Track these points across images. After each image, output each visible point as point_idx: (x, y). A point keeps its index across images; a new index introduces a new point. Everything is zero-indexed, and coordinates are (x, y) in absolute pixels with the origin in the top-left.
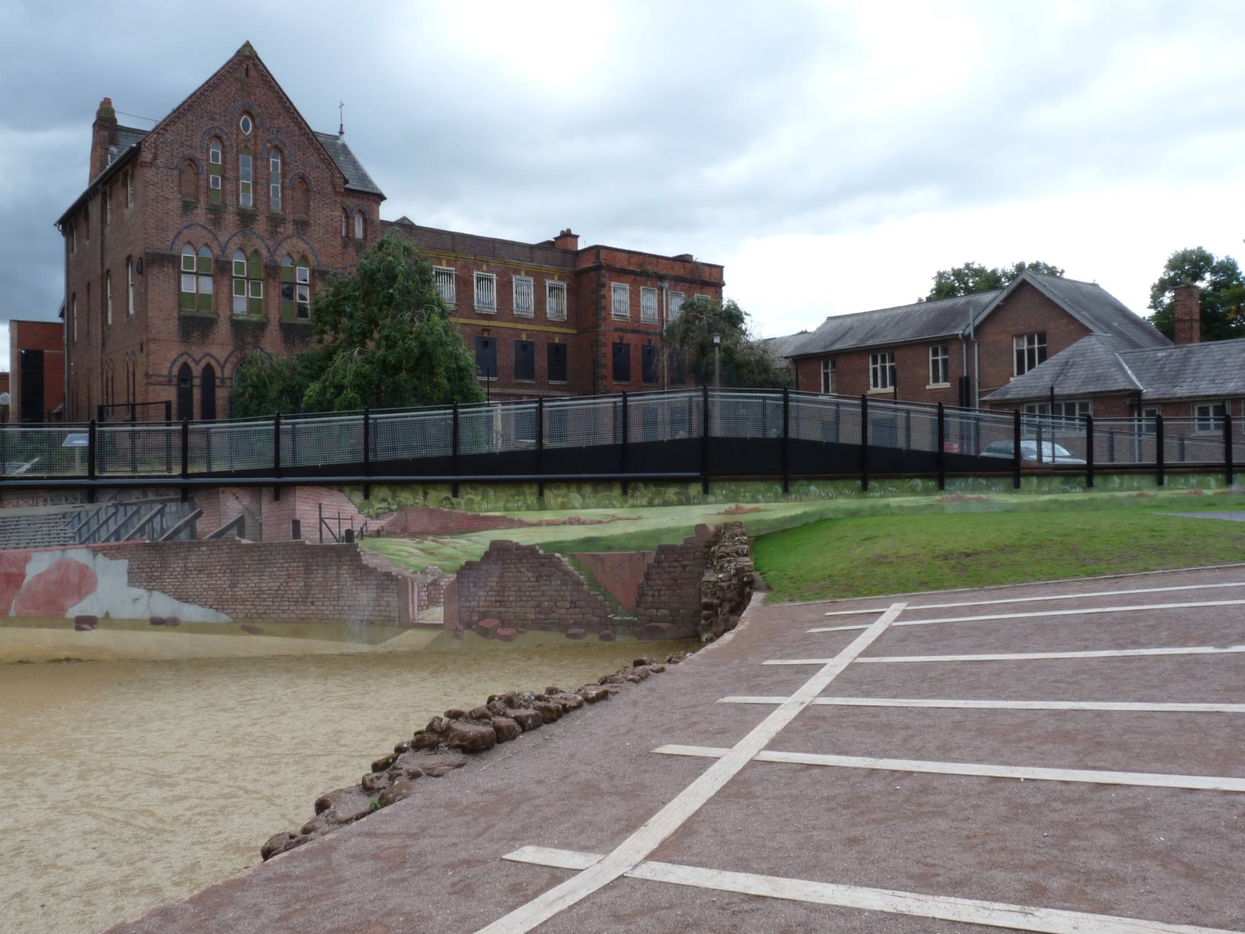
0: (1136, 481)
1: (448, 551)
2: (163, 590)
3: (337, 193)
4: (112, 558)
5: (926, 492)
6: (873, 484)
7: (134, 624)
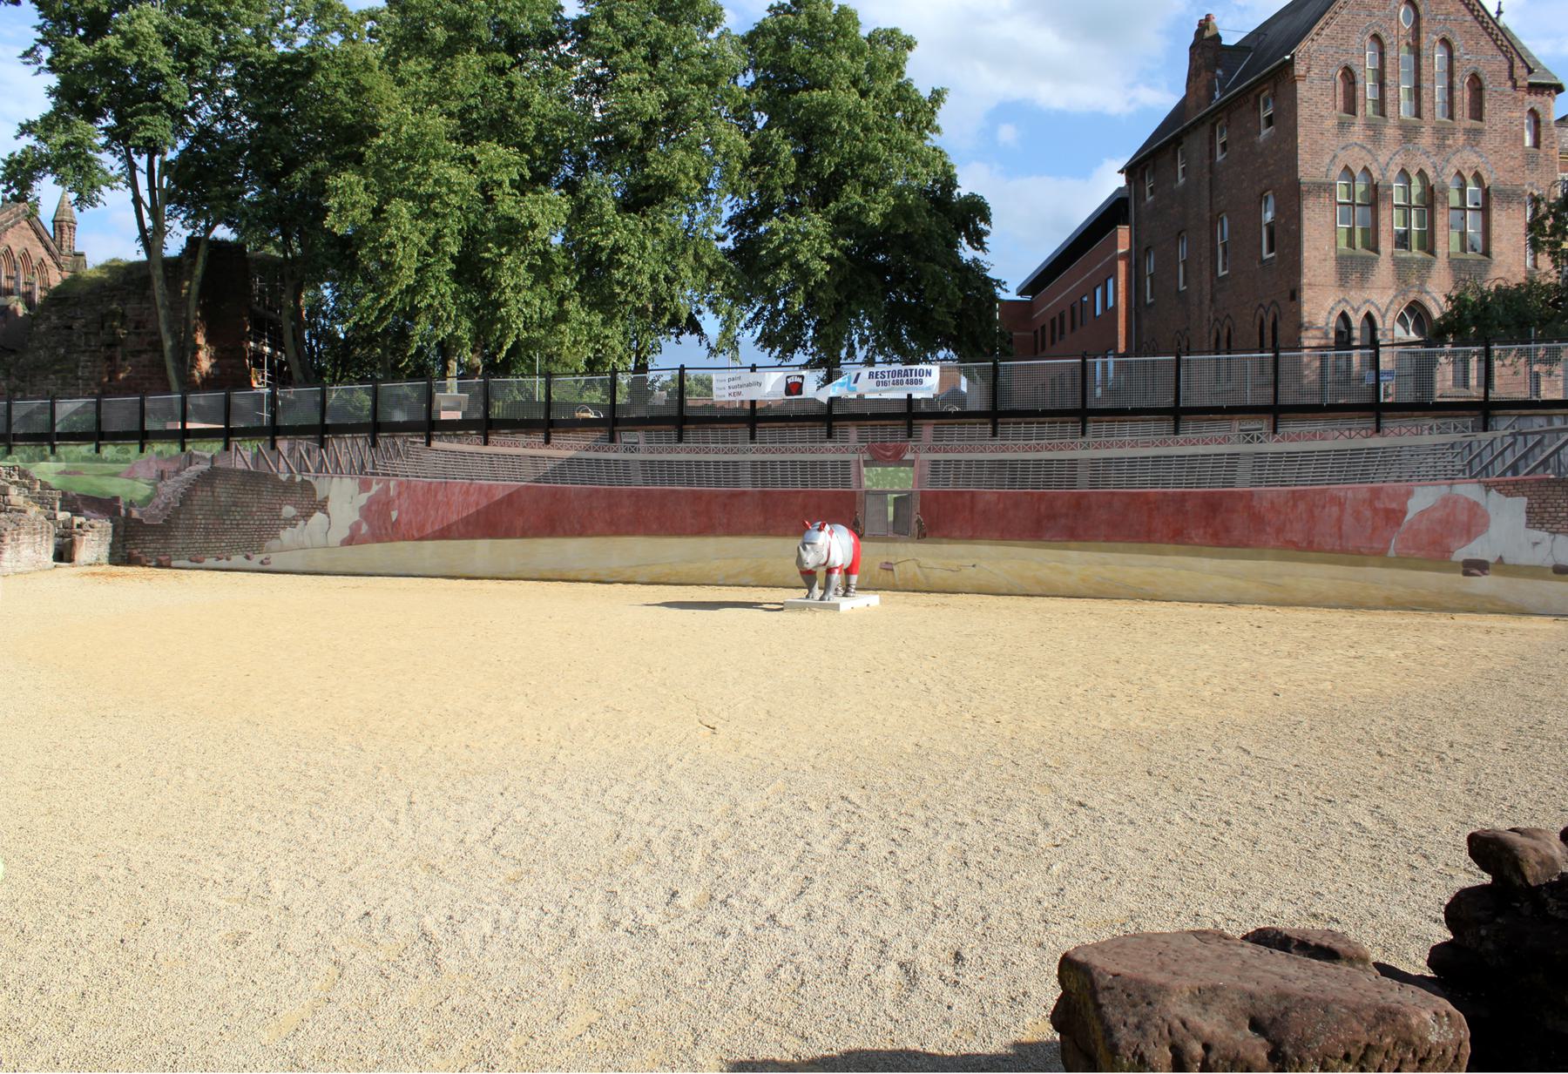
7: (1533, 572)
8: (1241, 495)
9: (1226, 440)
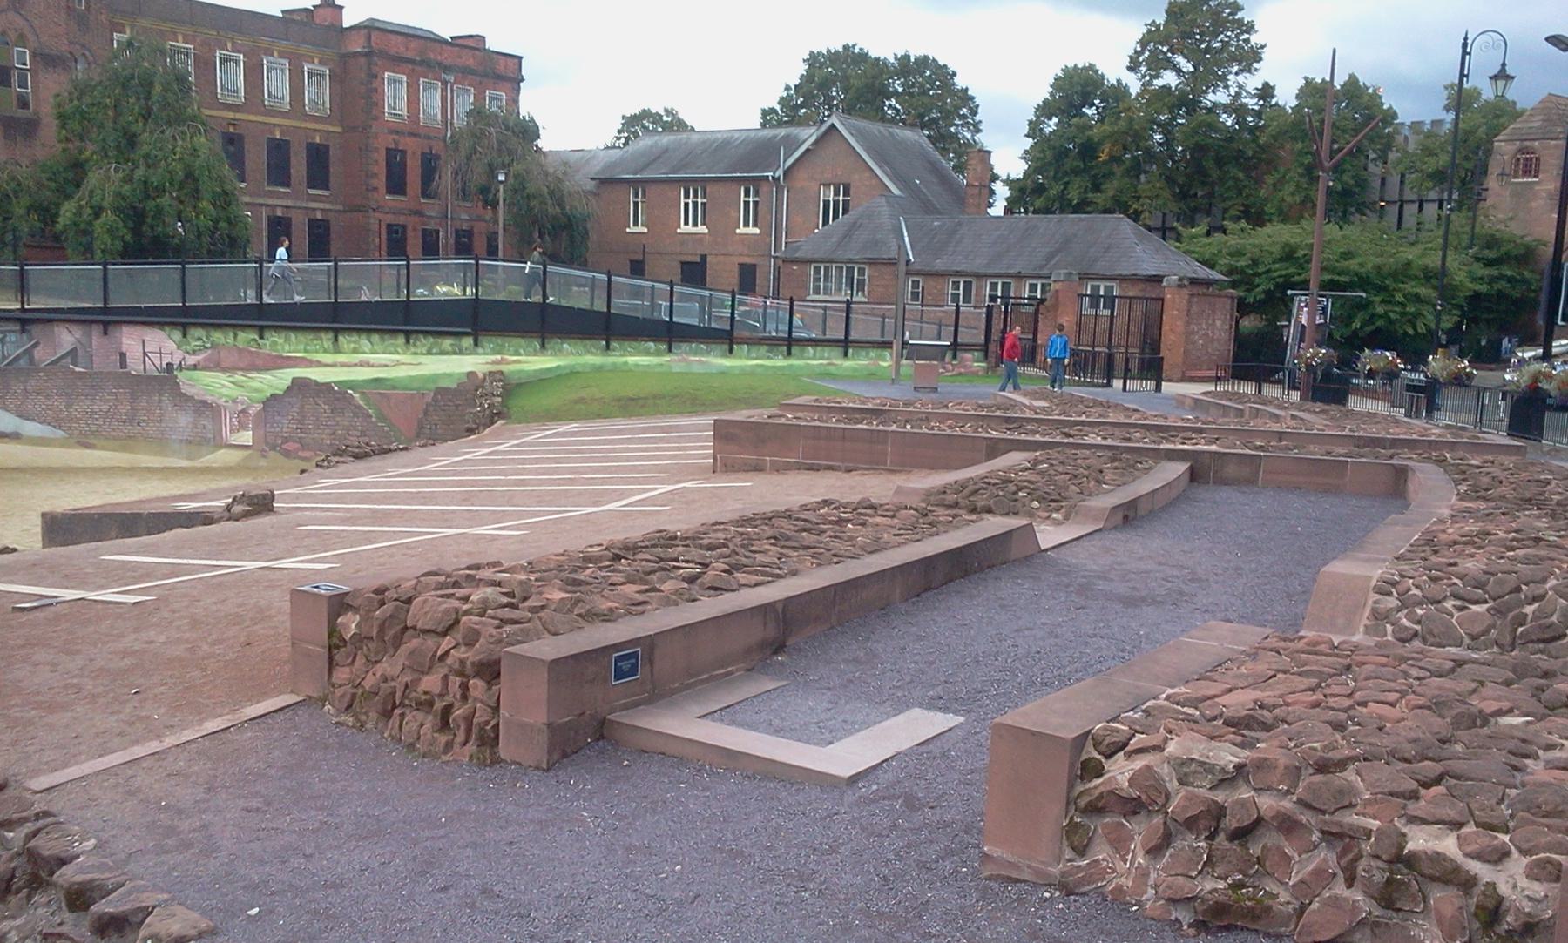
0: (826, 351)
1: (255, 384)
5: (658, 353)
6: (614, 344)
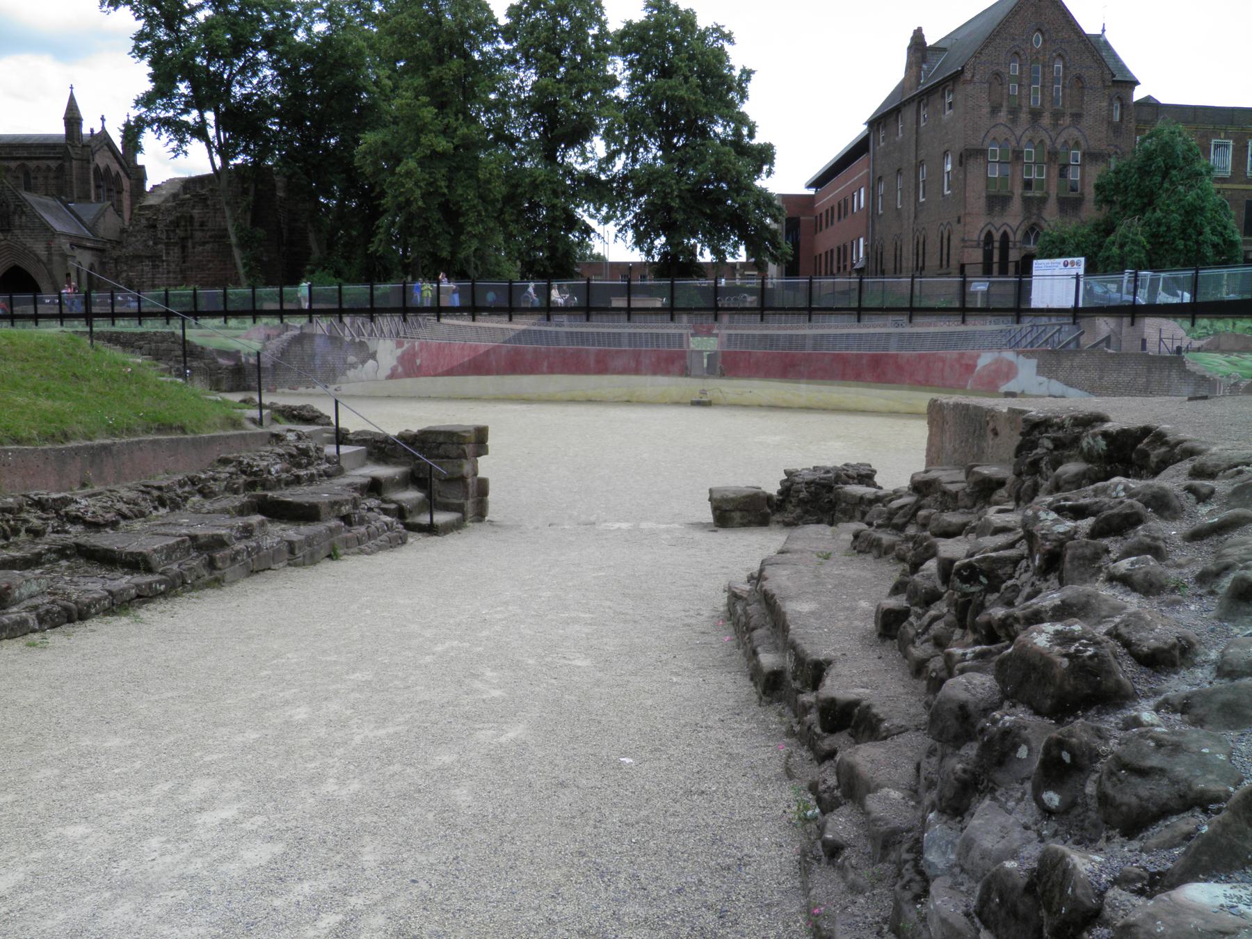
2: (1057, 379)
3: (1105, 87)
4: (1028, 357)
8: (892, 356)
9: (885, 326)
